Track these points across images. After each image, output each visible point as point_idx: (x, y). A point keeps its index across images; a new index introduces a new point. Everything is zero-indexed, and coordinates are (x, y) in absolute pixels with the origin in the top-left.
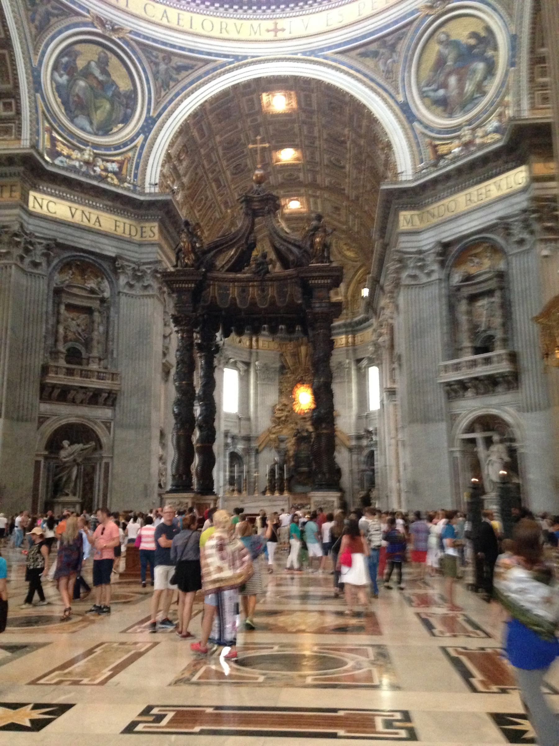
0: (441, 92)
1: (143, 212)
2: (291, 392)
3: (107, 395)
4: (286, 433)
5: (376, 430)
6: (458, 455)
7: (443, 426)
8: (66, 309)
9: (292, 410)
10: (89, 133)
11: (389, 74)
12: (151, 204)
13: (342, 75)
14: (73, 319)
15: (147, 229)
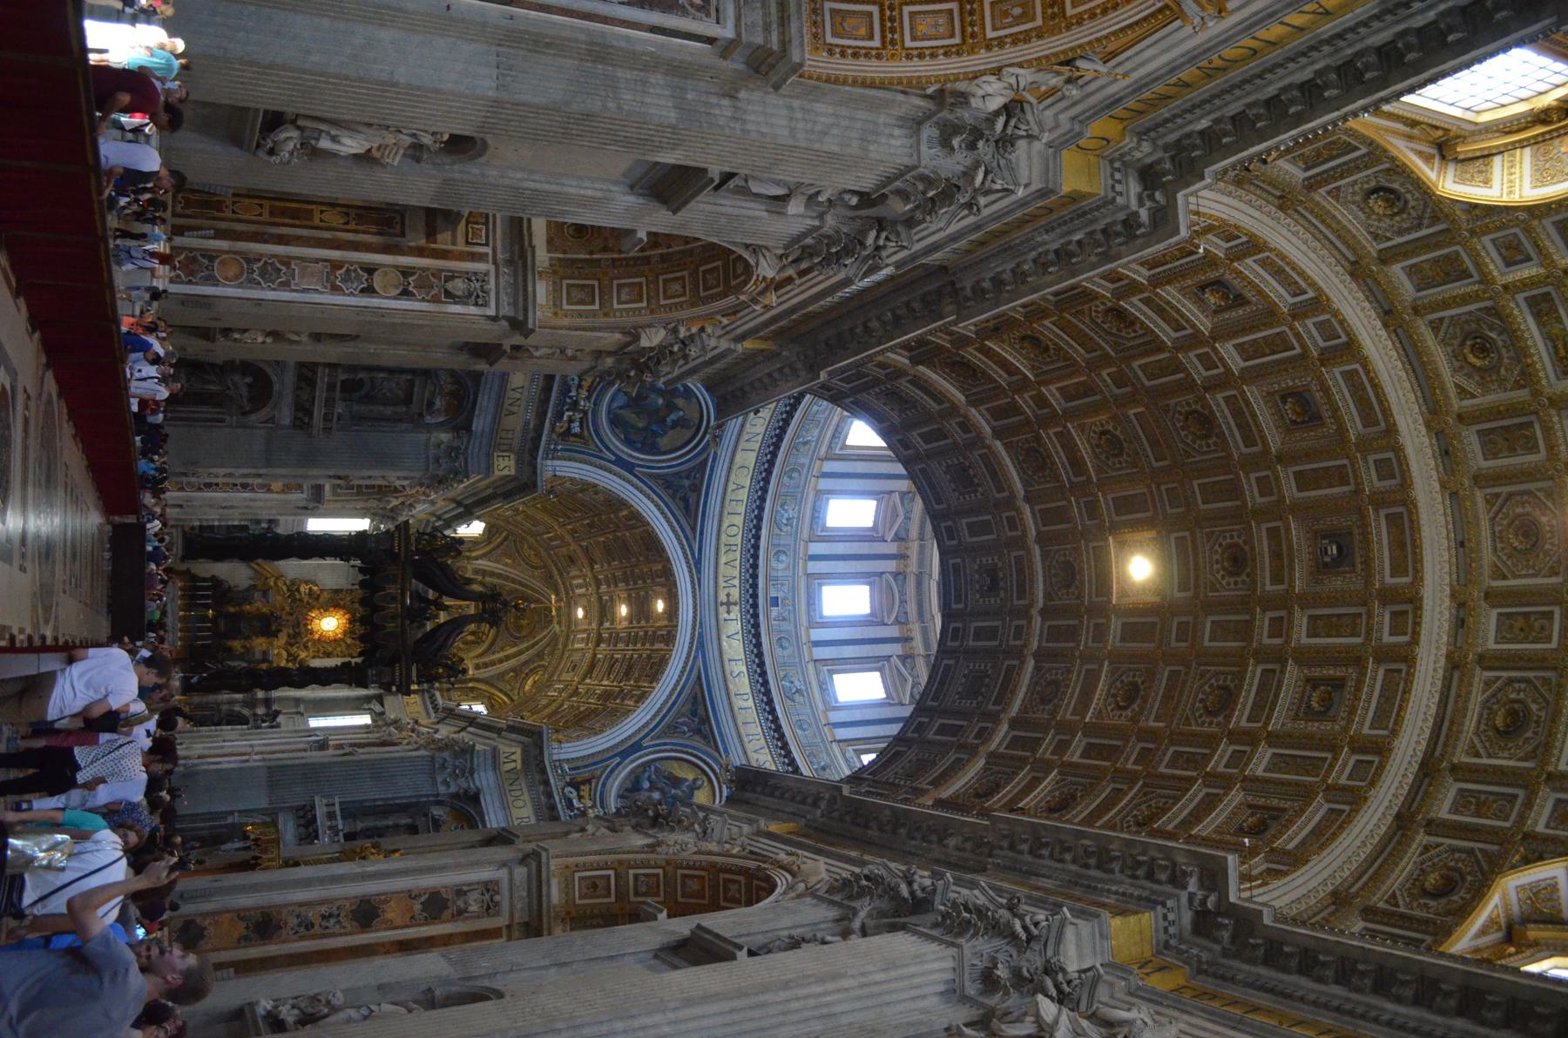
0: (646, 785)
1: (527, 458)
2: (337, 606)
3: (306, 421)
4: (276, 599)
5: (278, 726)
6: (230, 820)
7: (263, 803)
8: (407, 380)
9: (312, 608)
10: (609, 406)
11: (673, 729)
12: (534, 472)
13: (676, 677)
14: (397, 384)
15: (506, 463)
